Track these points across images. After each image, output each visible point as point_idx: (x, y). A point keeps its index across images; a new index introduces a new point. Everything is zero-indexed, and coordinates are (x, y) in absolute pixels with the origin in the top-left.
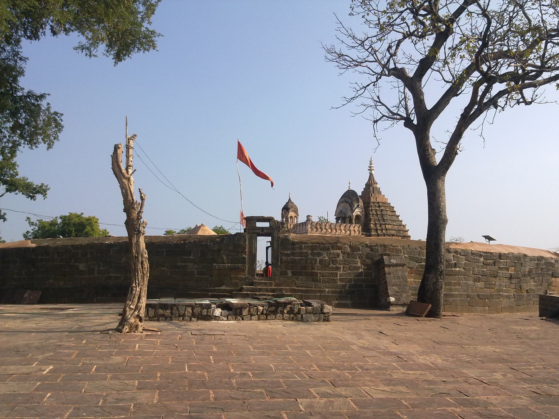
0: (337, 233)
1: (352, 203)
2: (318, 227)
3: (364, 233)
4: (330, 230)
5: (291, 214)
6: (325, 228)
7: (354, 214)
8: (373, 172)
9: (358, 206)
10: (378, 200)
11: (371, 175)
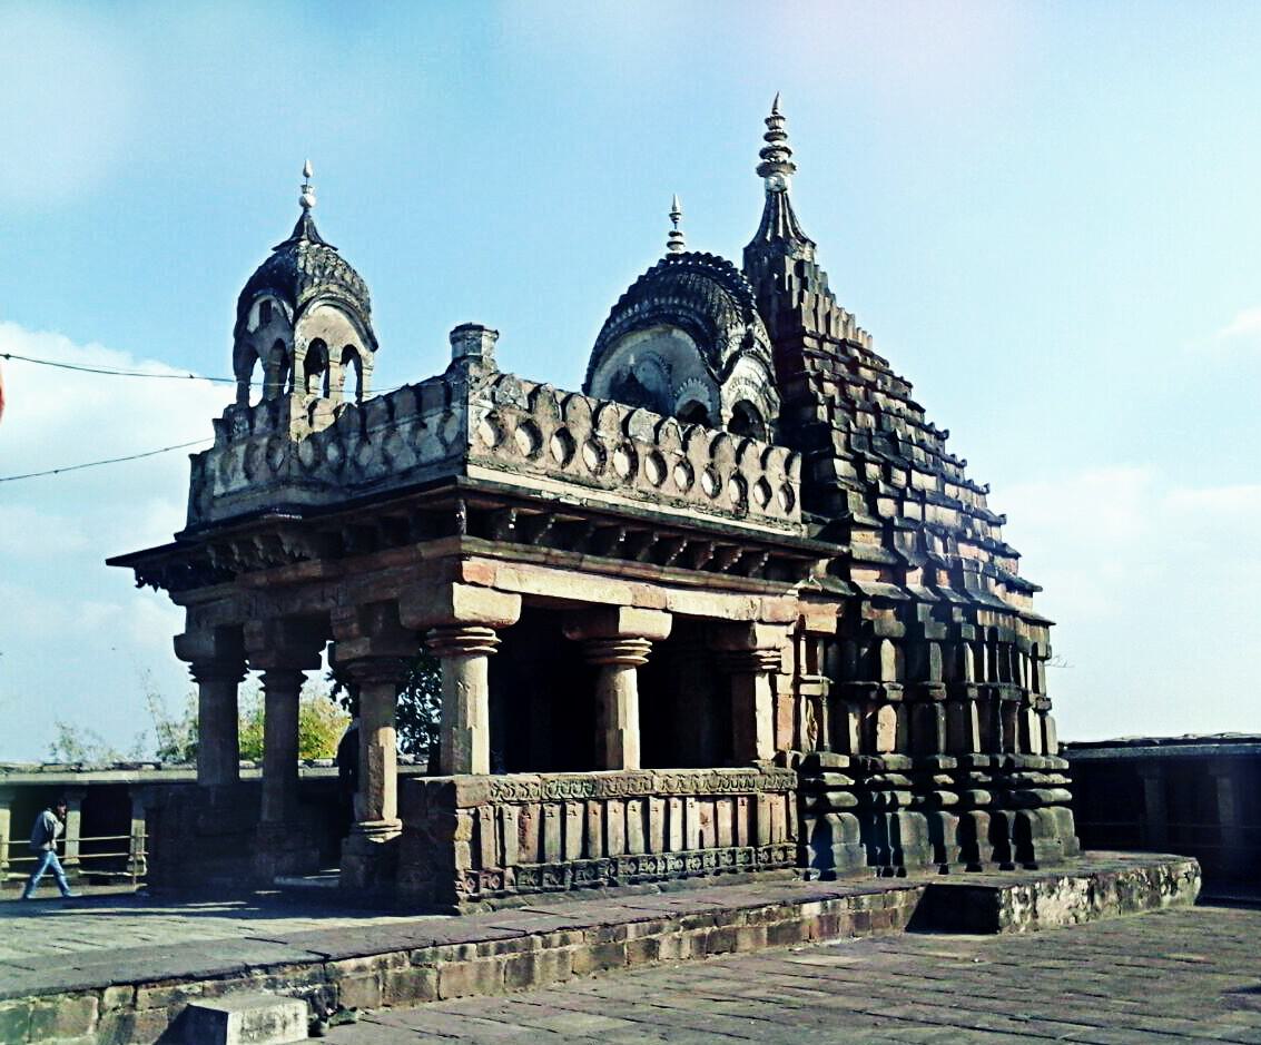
0: (668, 490)
1: (710, 320)
2: (548, 427)
3: (808, 514)
4: (621, 462)
5: (321, 321)
6: (593, 441)
7: (729, 394)
8: (789, 180)
9: (748, 341)
10: (837, 332)
11: (776, 201)
